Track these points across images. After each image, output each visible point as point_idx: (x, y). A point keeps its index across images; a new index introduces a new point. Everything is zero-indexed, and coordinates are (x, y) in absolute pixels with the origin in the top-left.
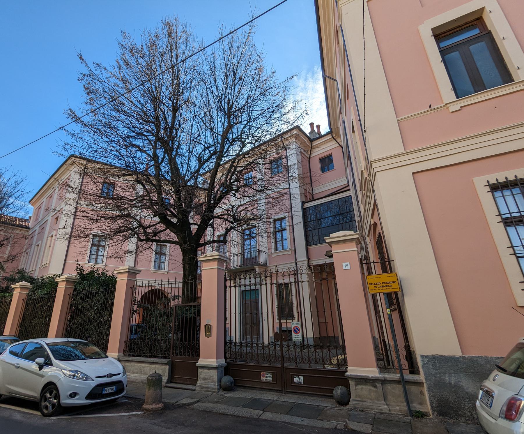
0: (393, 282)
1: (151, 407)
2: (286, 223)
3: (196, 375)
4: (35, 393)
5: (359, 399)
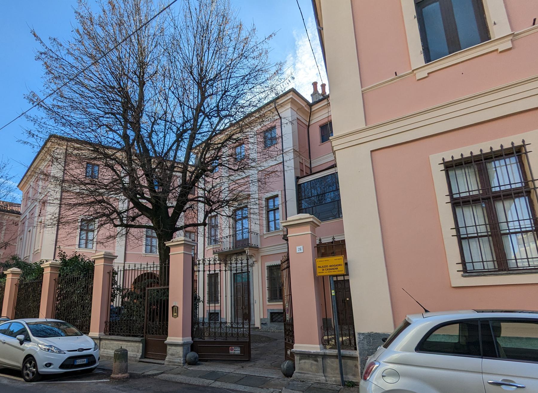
0: (339, 265)
1: (117, 376)
2: (279, 201)
3: (165, 351)
4: (18, 364)
5: (303, 372)
